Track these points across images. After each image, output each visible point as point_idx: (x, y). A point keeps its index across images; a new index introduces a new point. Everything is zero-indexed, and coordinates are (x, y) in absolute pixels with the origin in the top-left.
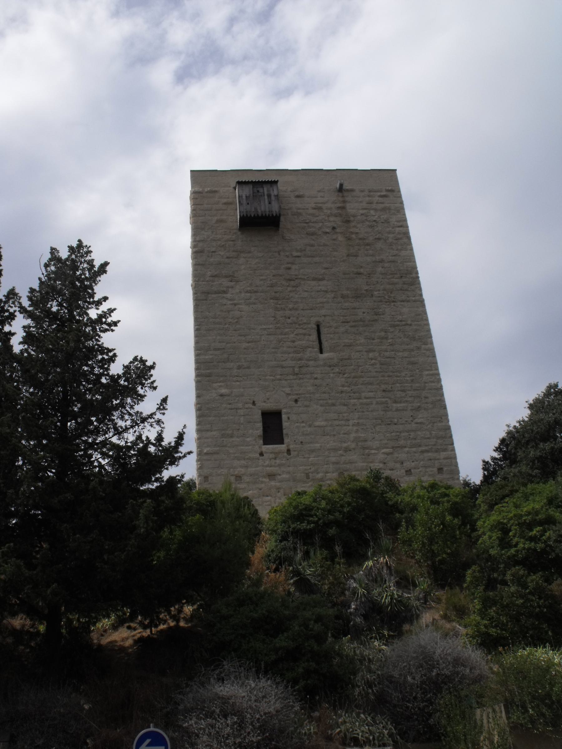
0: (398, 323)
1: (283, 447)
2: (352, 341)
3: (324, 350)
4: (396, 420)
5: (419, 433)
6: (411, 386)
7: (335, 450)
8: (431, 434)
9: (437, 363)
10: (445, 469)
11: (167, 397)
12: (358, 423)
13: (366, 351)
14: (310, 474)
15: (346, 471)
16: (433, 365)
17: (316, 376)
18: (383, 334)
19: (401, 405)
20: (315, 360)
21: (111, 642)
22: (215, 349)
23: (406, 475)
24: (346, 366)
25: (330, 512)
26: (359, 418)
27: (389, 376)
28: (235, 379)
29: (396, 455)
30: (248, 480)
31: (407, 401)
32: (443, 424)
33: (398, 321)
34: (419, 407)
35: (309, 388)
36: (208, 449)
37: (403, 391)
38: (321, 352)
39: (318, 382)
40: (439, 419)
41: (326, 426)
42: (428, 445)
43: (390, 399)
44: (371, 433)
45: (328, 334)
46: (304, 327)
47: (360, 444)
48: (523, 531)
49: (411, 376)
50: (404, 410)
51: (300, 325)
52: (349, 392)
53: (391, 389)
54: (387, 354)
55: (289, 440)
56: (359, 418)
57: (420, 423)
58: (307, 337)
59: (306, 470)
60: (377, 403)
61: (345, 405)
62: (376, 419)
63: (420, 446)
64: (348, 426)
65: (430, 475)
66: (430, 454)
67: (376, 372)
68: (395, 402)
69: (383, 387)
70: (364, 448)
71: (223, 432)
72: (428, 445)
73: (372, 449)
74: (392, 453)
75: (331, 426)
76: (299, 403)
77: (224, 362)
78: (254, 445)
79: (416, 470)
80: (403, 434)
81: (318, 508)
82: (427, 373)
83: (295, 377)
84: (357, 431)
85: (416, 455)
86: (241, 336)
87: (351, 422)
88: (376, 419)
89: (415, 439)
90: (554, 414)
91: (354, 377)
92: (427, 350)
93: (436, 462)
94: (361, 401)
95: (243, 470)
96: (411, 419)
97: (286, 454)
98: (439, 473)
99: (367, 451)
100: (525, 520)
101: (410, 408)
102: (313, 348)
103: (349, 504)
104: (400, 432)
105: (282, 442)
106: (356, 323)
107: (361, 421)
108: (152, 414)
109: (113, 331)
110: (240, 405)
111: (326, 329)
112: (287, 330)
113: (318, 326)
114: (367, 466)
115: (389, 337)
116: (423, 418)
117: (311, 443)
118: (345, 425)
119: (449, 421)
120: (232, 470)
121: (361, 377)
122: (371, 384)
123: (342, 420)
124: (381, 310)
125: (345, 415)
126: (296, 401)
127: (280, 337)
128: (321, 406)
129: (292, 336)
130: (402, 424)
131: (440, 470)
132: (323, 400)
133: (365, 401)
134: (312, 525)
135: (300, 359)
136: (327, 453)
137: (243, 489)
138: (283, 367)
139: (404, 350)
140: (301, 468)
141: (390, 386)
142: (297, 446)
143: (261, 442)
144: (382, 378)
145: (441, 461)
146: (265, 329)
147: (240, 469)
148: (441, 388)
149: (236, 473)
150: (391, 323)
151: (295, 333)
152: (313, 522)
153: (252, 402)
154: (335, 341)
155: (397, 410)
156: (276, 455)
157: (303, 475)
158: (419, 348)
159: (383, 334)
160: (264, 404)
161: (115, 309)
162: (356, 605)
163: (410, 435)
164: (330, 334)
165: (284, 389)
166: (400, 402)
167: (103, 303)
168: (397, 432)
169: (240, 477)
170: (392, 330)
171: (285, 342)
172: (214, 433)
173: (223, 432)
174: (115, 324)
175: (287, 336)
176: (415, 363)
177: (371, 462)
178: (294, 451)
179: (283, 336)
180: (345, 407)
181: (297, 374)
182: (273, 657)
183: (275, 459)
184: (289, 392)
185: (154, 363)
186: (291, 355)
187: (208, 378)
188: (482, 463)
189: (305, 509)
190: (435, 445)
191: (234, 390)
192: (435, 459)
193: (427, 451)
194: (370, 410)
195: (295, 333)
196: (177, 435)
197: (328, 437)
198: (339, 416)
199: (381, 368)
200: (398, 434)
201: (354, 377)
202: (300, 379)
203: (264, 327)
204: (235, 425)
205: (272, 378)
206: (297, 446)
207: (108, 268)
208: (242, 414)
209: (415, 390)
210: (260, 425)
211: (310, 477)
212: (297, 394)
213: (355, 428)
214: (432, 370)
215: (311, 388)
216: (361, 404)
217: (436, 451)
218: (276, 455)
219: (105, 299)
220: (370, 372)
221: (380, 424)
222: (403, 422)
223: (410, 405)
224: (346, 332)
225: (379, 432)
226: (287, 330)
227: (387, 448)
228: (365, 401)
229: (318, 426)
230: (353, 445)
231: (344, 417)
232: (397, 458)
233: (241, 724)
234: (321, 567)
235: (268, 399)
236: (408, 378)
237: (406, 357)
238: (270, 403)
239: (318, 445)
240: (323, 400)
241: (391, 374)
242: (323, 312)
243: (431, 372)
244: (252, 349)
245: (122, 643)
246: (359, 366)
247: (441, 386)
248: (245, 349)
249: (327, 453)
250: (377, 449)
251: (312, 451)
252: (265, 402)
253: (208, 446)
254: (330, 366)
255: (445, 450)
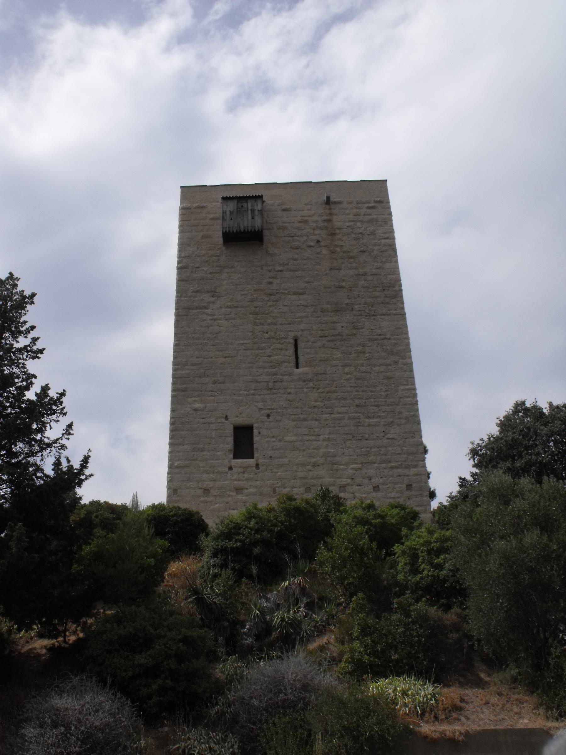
0: (377, 337)
1: (251, 462)
2: (329, 355)
3: (300, 365)
4: (367, 436)
5: (390, 449)
6: (386, 401)
7: (304, 465)
8: (402, 450)
9: (413, 378)
10: (414, 485)
11: (72, 423)
12: (328, 438)
13: (342, 366)
14: (277, 489)
15: (313, 486)
16: (410, 379)
17: (289, 391)
18: (360, 348)
19: (374, 420)
20: (290, 374)
21: (30, 649)
22: (192, 364)
23: (374, 490)
24: (321, 381)
25: (257, 531)
26: (330, 433)
27: (363, 391)
28: (209, 394)
29: (364, 471)
30: (215, 494)
31: (380, 417)
32: (416, 440)
33: (377, 335)
34: (392, 422)
35: (282, 403)
36: (179, 462)
37: (377, 406)
38: (297, 367)
39: (291, 397)
40: (411, 435)
41: (296, 441)
42: (399, 461)
43: (363, 414)
44: (341, 448)
45: (304, 348)
46: (282, 342)
47: (329, 459)
48: (431, 558)
49: (386, 391)
50: (376, 425)
51: (277, 339)
52: (321, 407)
53: (364, 404)
54: (363, 369)
55: (258, 455)
56: (330, 433)
57: (393, 439)
58: (283, 352)
59: (273, 484)
60: (349, 418)
61: (316, 420)
62: (347, 434)
63: (390, 462)
64: (319, 441)
65: (397, 492)
66: (399, 470)
67: (351, 387)
68: (368, 417)
69: (357, 402)
70: (333, 464)
71: (195, 446)
72: (399, 461)
73: (341, 465)
74: (360, 469)
75: (301, 440)
76: (271, 418)
77: (200, 377)
78: (224, 459)
79: (384, 486)
80: (373, 450)
81: (246, 527)
82: (402, 387)
83: (269, 392)
84: (327, 446)
85: (385, 470)
86: (219, 351)
87: (321, 438)
88: (347, 434)
89: (386, 455)
90: (514, 433)
91: (328, 392)
92: (405, 364)
93: (406, 478)
94: (333, 416)
95: (211, 484)
96: (383, 434)
97: (254, 468)
98: (407, 490)
99: (336, 466)
100: (433, 547)
101: (382, 423)
102: (289, 363)
103: (282, 523)
104: (371, 448)
105: (253, 458)
106: (334, 338)
107: (331, 436)
108: (58, 439)
109: (39, 358)
110: (213, 420)
111: (303, 344)
112: (264, 345)
113: (296, 341)
114: (334, 481)
115: (367, 352)
116: (395, 433)
117: (280, 457)
118: (315, 440)
119: (422, 437)
120: (200, 483)
121: (335, 392)
122: (345, 399)
123: (313, 435)
124: (360, 324)
125: (316, 430)
126: (268, 416)
127: (256, 351)
128: (293, 421)
129: (269, 350)
130: (373, 440)
131: (409, 487)
132: (294, 414)
133: (337, 416)
134: (238, 544)
135: (275, 374)
136: (295, 468)
137: (210, 502)
138: (257, 382)
139: (381, 365)
140: (268, 482)
141: (364, 401)
142: (265, 461)
143: (232, 456)
144: (356, 393)
145: (410, 477)
146: (242, 344)
147: (209, 483)
148: (416, 403)
149: (205, 486)
150: (369, 337)
151: (272, 348)
152: (240, 541)
153: (224, 416)
154: (311, 356)
155: (369, 425)
156: (245, 469)
157: (269, 489)
158: (396, 363)
159: (360, 348)
160: (237, 419)
161: (38, 338)
162: (250, 626)
163: (381, 451)
164: (307, 348)
165: (256, 404)
166: (373, 418)
167: (31, 331)
168: (368, 447)
169: (208, 490)
170: (370, 344)
171: (261, 357)
172: (186, 447)
173: (195, 446)
174: (41, 351)
175: (264, 351)
176: (391, 378)
177: (339, 478)
178: (263, 465)
179: (260, 351)
180: (317, 422)
181: (271, 389)
182: (130, 674)
183: (244, 473)
184: (262, 407)
185: (64, 391)
186: (266, 370)
187: (183, 393)
188: (458, 480)
189: (235, 528)
190: (405, 461)
191: (208, 405)
192: (404, 475)
193: (397, 467)
194: (342, 425)
195: (272, 348)
196: (82, 458)
197: (298, 452)
198: (310, 431)
199: (356, 383)
200: (368, 449)
201: (328, 392)
202: (273, 394)
203: (242, 342)
204: (206, 440)
205: (246, 392)
206: (265, 461)
207: (35, 299)
208: (214, 428)
209: (388, 405)
210: (231, 440)
211: (277, 491)
212: (269, 409)
213: (325, 443)
214: (408, 385)
215: (283, 403)
216: (334, 419)
217: (406, 468)
218: (245, 469)
219: (33, 328)
220: (345, 386)
221: (351, 440)
222: (375, 437)
223: (383, 420)
224: (323, 346)
225: (349, 447)
226: (264, 345)
227: (356, 463)
228: (337, 416)
229: (288, 441)
230: (322, 461)
231: (315, 432)
232: (366, 473)
233: (65, 737)
234: (224, 586)
235: (241, 414)
236: (383, 393)
237: (382, 372)
238: (243, 417)
239: (287, 460)
240: (294, 414)
241: (365, 389)
242: (301, 326)
243: (407, 387)
244: (229, 364)
245: (39, 651)
246: (334, 381)
247: (417, 401)
248: (221, 364)
249: (295, 468)
250: (346, 464)
251: (281, 466)
252: (237, 416)
253: (178, 460)
254: (304, 381)
255: (415, 466)
